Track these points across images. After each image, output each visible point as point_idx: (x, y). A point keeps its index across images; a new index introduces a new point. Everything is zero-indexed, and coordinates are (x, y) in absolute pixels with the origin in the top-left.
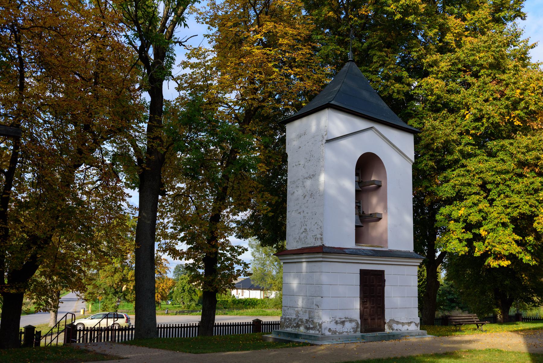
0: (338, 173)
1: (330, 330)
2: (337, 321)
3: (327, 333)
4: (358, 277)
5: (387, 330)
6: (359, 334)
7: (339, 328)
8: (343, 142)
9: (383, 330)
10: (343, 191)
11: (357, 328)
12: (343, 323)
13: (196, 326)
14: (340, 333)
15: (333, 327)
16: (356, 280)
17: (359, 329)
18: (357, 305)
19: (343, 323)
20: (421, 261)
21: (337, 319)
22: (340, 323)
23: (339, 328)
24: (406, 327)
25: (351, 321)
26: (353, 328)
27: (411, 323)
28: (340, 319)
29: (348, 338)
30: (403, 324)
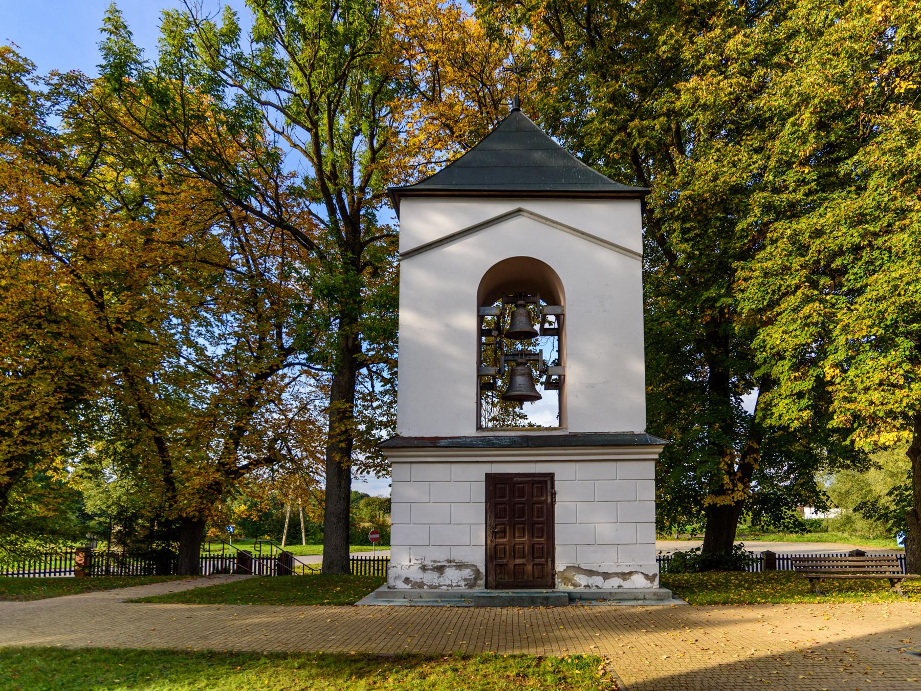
0: (441, 305)
1: (407, 580)
2: (424, 566)
3: (400, 585)
4: (483, 486)
5: (562, 587)
6: (480, 590)
7: (430, 578)
8: (453, 248)
9: (553, 585)
10: (453, 335)
11: (476, 579)
12: (440, 569)
13: (234, 558)
14: (431, 587)
15: (416, 575)
16: (479, 491)
17: (482, 582)
18: (480, 536)
19: (440, 569)
20: (661, 450)
21: (428, 563)
22: (431, 570)
23: (430, 578)
24: (615, 582)
25: (460, 566)
26: (465, 580)
27: (631, 573)
28: (435, 562)
29: (459, 600)
30: (606, 576)
